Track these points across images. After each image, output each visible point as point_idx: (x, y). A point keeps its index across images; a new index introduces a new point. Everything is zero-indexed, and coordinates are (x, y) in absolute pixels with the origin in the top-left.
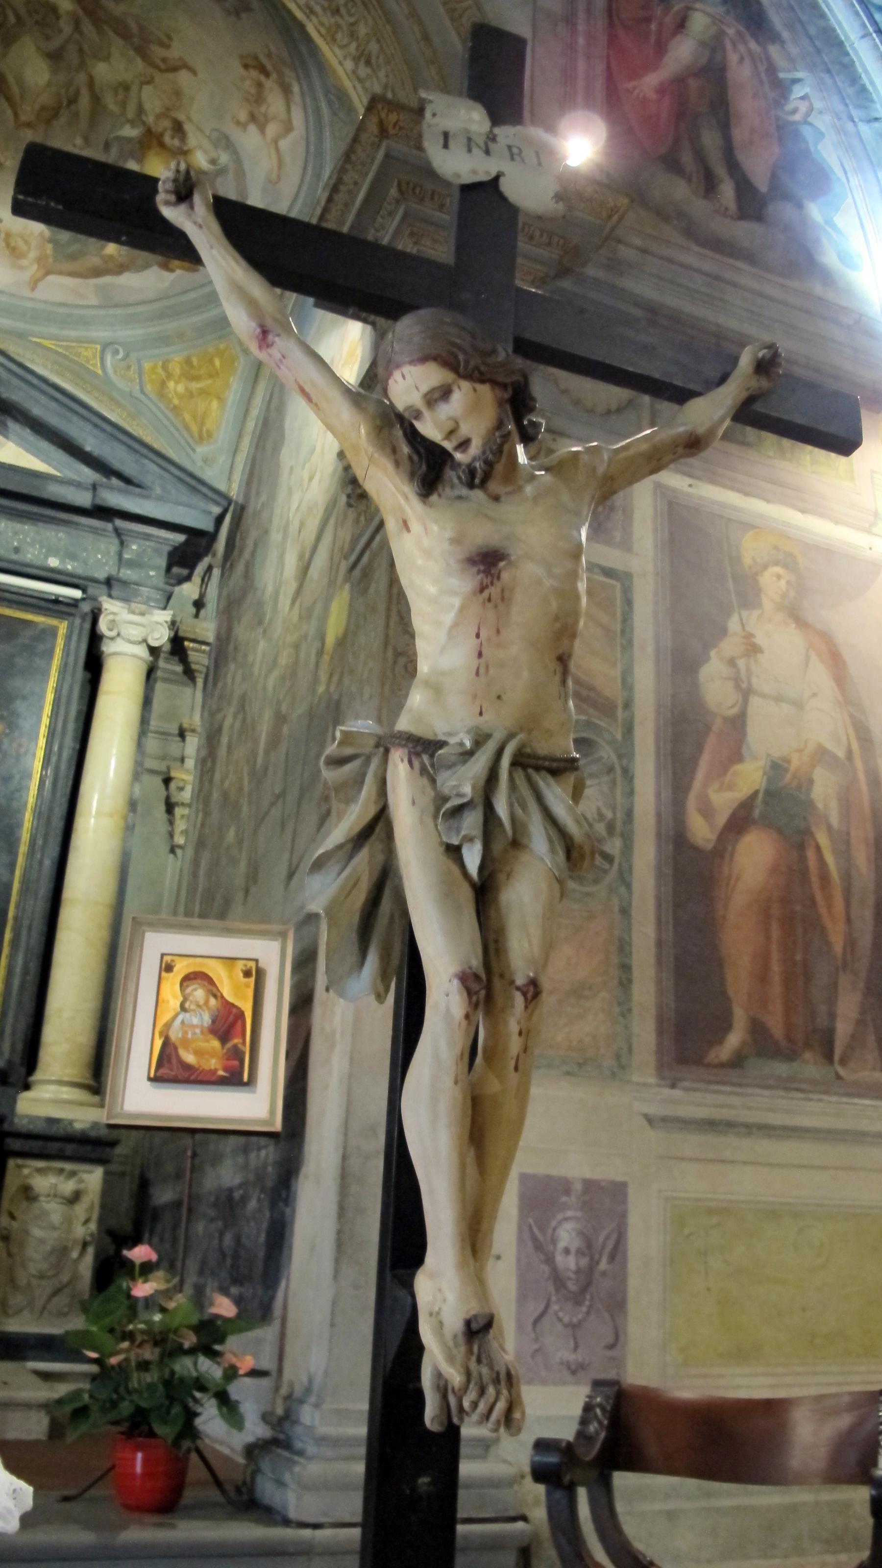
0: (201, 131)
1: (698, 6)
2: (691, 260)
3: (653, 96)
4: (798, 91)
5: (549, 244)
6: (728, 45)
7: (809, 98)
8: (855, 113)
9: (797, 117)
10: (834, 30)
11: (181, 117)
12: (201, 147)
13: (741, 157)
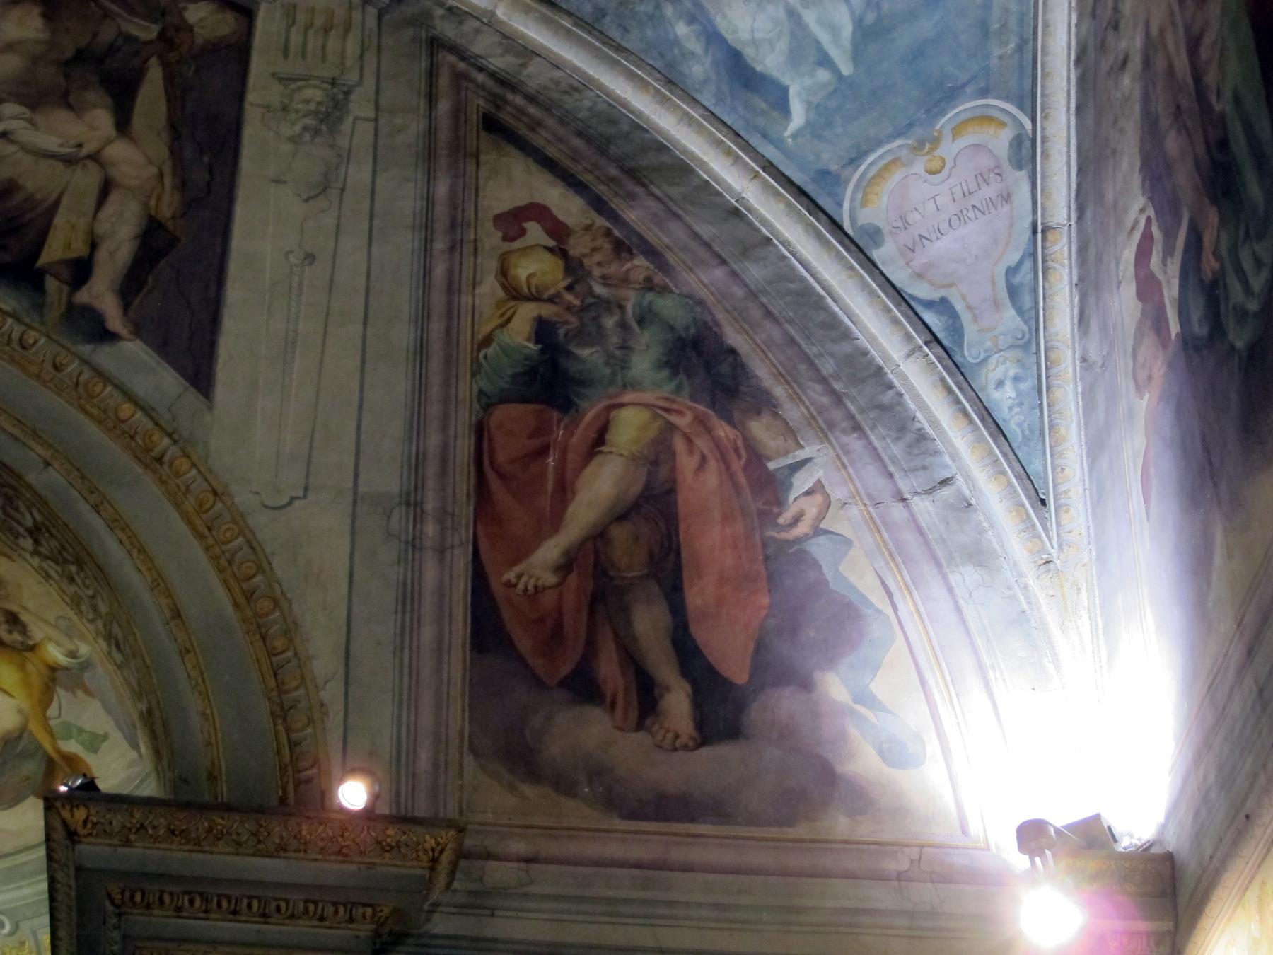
0: (46, 622)
1: (627, 398)
2: (614, 849)
3: (551, 579)
4: (802, 482)
5: (351, 920)
6: (679, 444)
7: (828, 489)
8: (904, 485)
9: (802, 529)
10: (865, 353)
11: (14, 608)
12: (50, 640)
13: (700, 633)
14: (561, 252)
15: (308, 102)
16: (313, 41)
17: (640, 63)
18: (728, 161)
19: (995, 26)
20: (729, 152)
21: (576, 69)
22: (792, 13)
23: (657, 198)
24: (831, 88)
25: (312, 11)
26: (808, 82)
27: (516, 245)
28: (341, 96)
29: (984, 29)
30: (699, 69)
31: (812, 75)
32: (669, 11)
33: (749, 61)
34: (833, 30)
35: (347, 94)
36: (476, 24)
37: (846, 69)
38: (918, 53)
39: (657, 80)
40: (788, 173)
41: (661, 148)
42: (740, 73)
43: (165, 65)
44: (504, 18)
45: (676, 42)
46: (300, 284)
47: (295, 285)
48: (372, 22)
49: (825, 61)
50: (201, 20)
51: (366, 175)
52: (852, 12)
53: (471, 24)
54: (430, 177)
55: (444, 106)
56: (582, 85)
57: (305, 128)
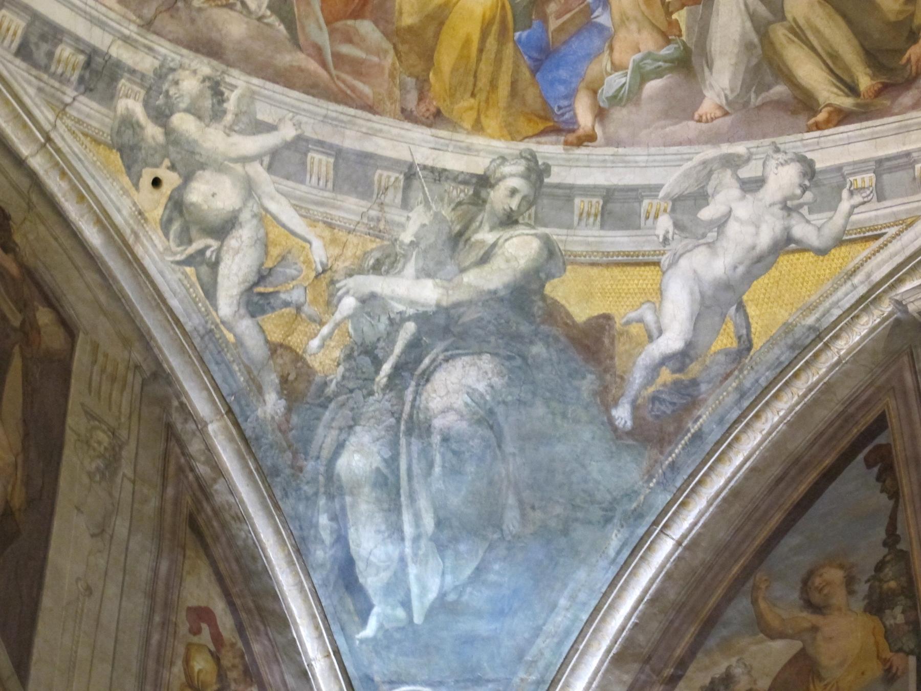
14: (217, 659)
15: (100, 443)
16: (105, 388)
17: (285, 523)
18: (315, 634)
19: (528, 658)
20: (317, 627)
21: (242, 501)
22: (402, 559)
23: (270, 640)
24: (401, 625)
25: (106, 355)
26: (389, 611)
27: (195, 639)
28: (117, 449)
29: (520, 656)
30: (321, 554)
31: (394, 608)
32: (322, 501)
33: (357, 571)
34: (424, 589)
35: (121, 448)
36: (194, 427)
37: (418, 619)
38: (470, 640)
39: (292, 545)
40: (346, 664)
41: (275, 597)
42: (347, 574)
43: (24, 358)
44: (211, 433)
45: (315, 526)
46: (82, 611)
47: (79, 611)
48: (137, 388)
49: (406, 604)
50: (47, 325)
51: (125, 532)
52: (442, 586)
53: (191, 426)
54: (158, 557)
55: (170, 491)
56: (242, 518)
57: (98, 469)
